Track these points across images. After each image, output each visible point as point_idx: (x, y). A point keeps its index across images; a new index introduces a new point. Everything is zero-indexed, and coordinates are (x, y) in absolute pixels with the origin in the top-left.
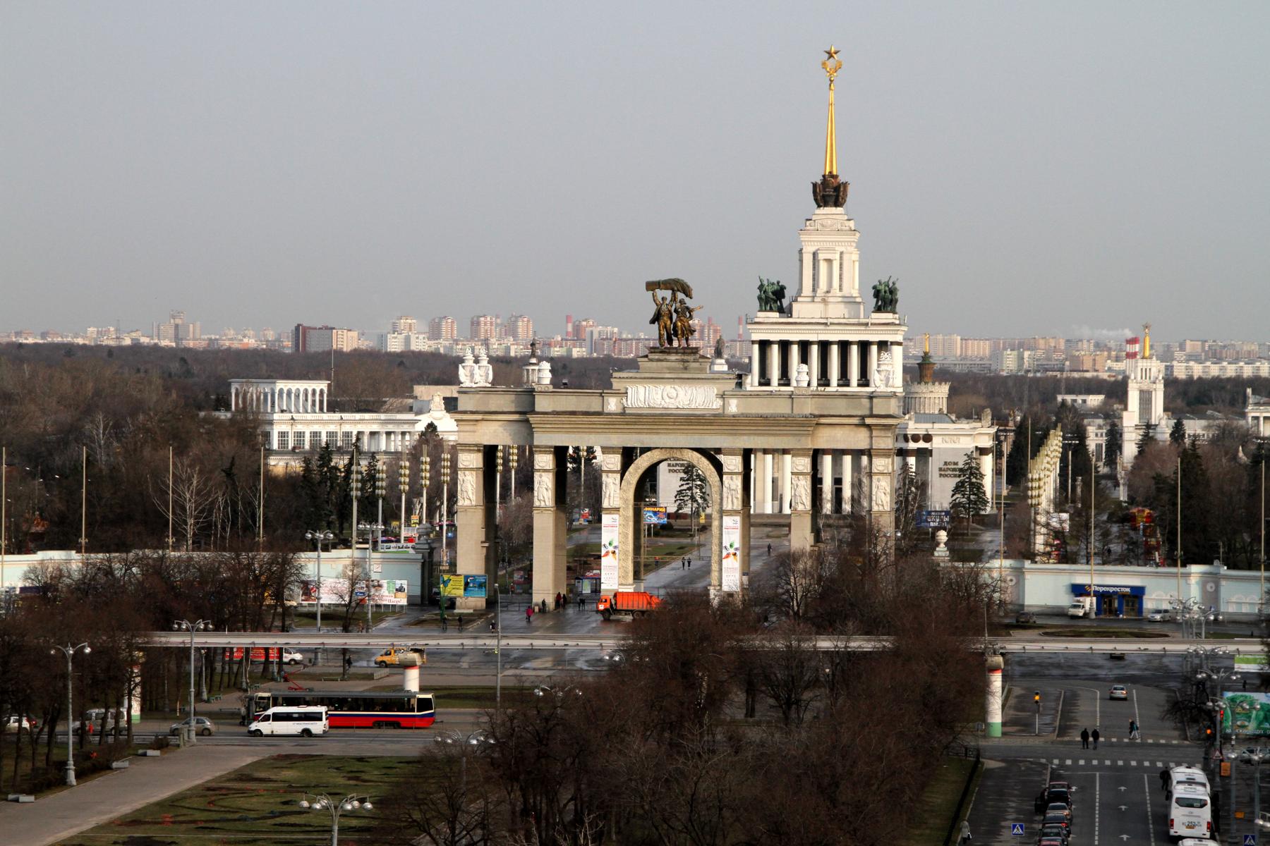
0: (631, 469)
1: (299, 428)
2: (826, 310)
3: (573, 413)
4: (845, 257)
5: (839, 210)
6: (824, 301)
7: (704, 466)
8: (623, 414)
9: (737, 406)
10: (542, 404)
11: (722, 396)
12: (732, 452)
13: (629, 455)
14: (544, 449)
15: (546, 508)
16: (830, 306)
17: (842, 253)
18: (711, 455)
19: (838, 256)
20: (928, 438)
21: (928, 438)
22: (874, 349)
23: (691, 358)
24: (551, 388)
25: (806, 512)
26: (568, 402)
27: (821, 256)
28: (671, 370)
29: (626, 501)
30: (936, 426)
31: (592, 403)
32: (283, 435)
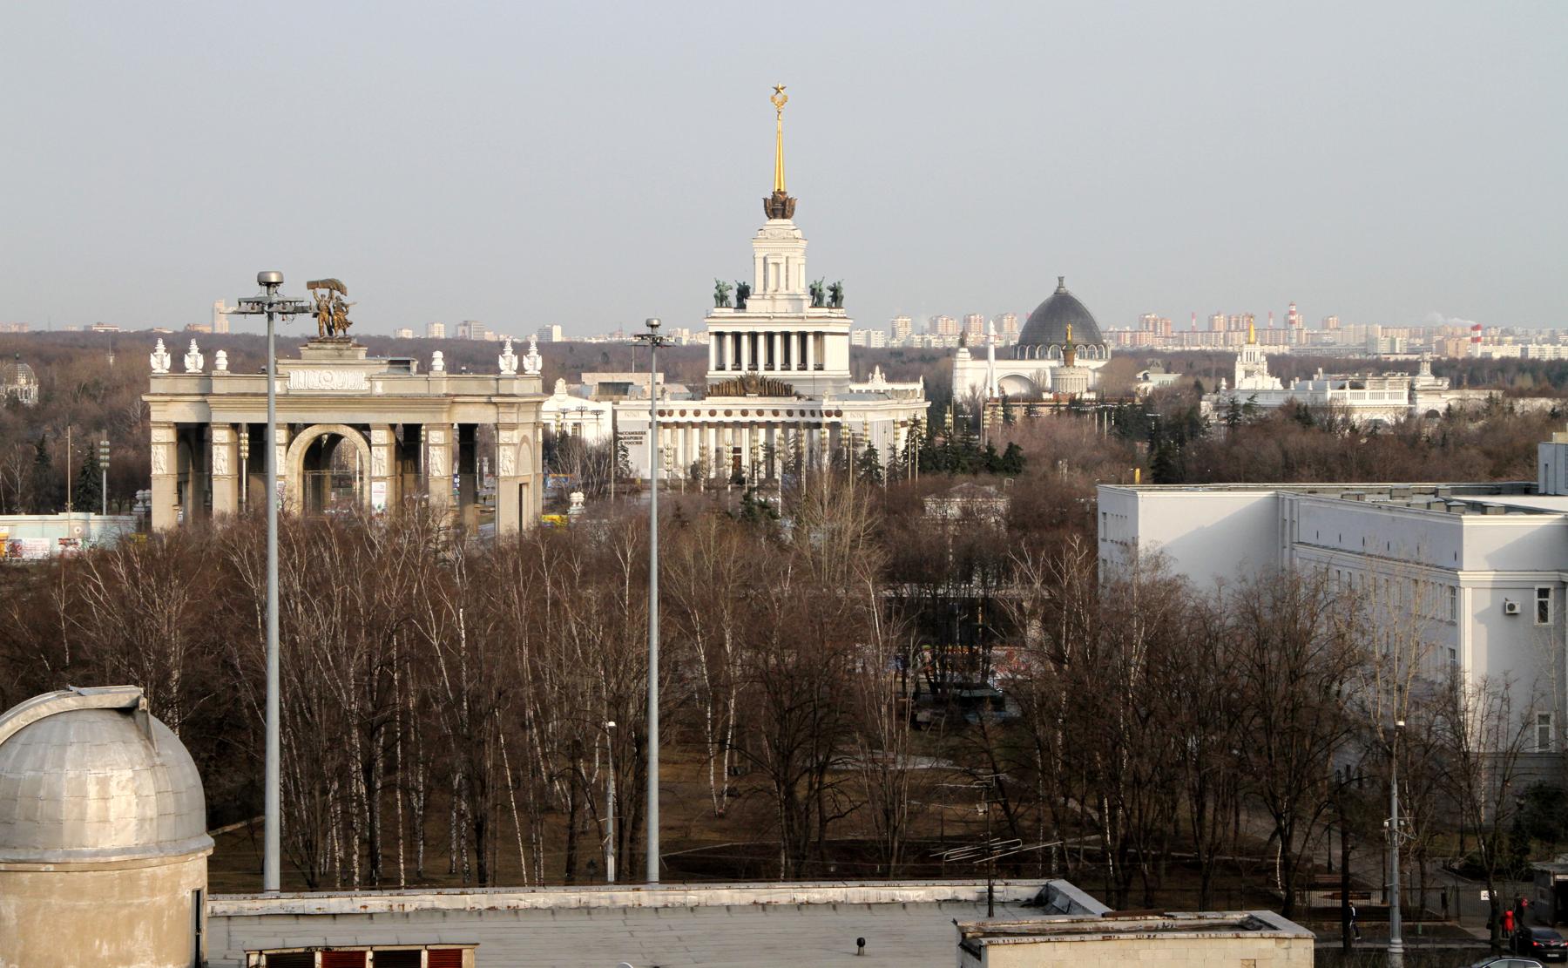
3: (244, 395)
5: (786, 221)
6: (773, 298)
8: (286, 395)
10: (219, 387)
11: (370, 379)
12: (379, 427)
14: (222, 426)
15: (223, 477)
18: (364, 429)
20: (839, 413)
21: (839, 413)
22: (810, 339)
23: (344, 346)
24: (228, 373)
25: (442, 478)
26: (243, 385)
27: (770, 261)
28: (328, 357)
29: (291, 469)
31: (259, 385)
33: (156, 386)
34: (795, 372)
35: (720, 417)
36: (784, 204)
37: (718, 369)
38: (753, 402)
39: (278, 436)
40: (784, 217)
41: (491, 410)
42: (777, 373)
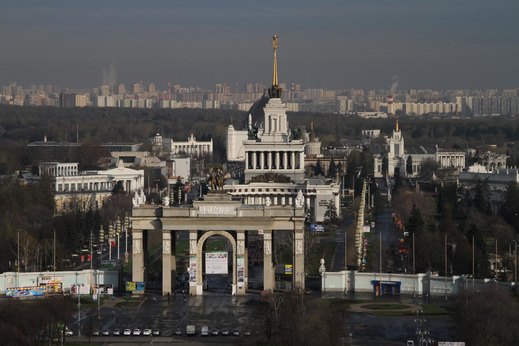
0: (201, 239)
1: (67, 182)
2: (274, 139)
3: (178, 217)
4: (281, 118)
5: (279, 99)
6: (273, 135)
7: (230, 237)
8: (198, 217)
9: (242, 214)
10: (165, 213)
11: (236, 210)
12: (241, 232)
13: (200, 233)
14: (167, 231)
15: (168, 255)
16: (276, 137)
17: (280, 116)
19: (278, 117)
20: (314, 191)
21: (314, 191)
23: (224, 195)
24: (169, 207)
25: (269, 255)
27: (272, 118)
28: (216, 199)
29: (199, 251)
30: (318, 186)
31: (186, 213)
32: (60, 185)
33: (135, 213)
34: (285, 170)
35: (257, 192)
36: (278, 91)
37: (249, 168)
38: (272, 185)
39: (193, 236)
40: (278, 97)
41: (292, 223)
42: (278, 170)
